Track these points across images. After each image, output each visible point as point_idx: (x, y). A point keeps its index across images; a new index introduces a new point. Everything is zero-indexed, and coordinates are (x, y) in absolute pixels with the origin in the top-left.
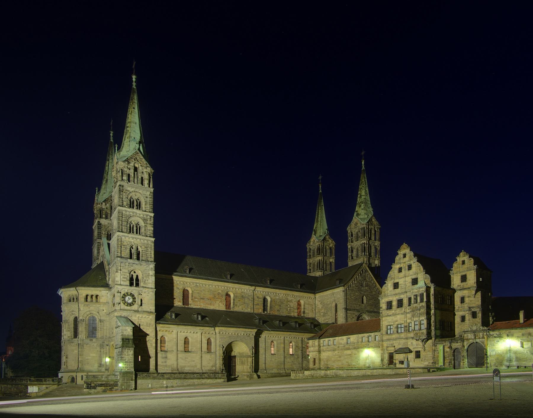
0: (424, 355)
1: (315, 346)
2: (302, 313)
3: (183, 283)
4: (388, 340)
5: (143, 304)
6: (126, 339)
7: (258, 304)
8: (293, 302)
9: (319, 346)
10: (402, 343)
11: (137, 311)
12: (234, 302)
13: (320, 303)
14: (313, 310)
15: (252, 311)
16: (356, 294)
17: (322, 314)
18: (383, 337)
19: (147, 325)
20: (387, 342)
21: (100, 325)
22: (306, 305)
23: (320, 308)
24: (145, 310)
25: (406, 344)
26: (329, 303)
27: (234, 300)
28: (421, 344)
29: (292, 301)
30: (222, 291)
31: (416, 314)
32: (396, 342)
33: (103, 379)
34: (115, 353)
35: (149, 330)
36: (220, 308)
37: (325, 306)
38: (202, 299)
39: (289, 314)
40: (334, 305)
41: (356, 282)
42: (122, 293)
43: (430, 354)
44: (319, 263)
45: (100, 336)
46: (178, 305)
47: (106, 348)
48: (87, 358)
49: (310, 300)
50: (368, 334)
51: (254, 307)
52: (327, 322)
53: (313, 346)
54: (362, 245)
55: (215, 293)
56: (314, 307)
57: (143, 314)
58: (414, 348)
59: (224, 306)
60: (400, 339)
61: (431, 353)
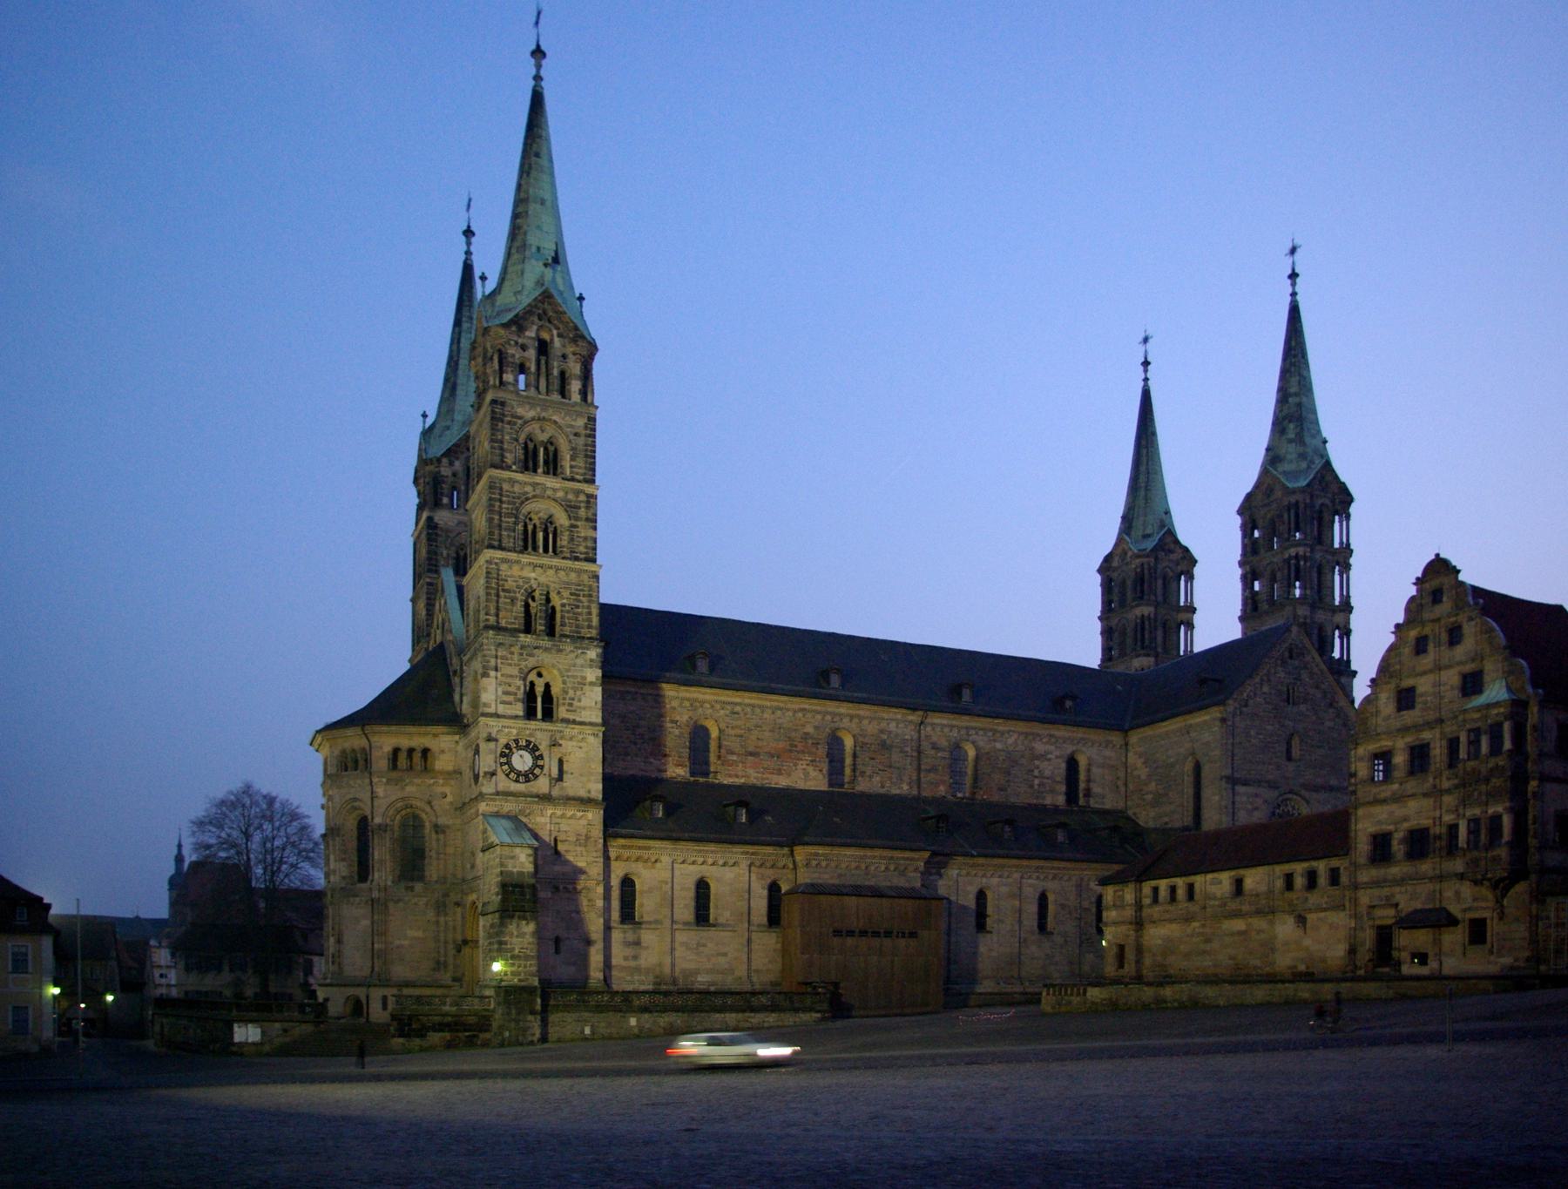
0: (1498, 934)
1: (1122, 907)
3: (692, 705)
4: (1376, 883)
5: (565, 776)
6: (516, 886)
7: (933, 769)
8: (1049, 760)
9: (1139, 906)
10: (1423, 895)
11: (546, 798)
12: (854, 765)
13: (1142, 760)
14: (1120, 783)
15: (915, 792)
16: (1269, 727)
17: (1149, 797)
18: (1359, 873)
19: (578, 842)
20: (1369, 891)
21: (434, 844)
22: (1094, 770)
23: (1143, 777)
24: (571, 793)
25: (1438, 896)
27: (855, 756)
28: (1490, 896)
29: (1049, 756)
30: (816, 728)
31: (1476, 794)
32: (1403, 889)
33: (447, 1008)
34: (481, 928)
35: (584, 858)
36: (809, 783)
38: (751, 754)
39: (1037, 798)
40: (1189, 766)
41: (1266, 689)
42: (503, 741)
43: (1520, 931)
44: (1139, 628)
45: (435, 877)
46: (674, 775)
47: (455, 913)
48: (397, 942)
49: (1108, 753)
51: (923, 780)
52: (1166, 823)
53: (1118, 903)
54: (1287, 561)
55: (793, 734)
56: (1121, 774)
57: (565, 804)
58: (1465, 910)
59: (821, 777)
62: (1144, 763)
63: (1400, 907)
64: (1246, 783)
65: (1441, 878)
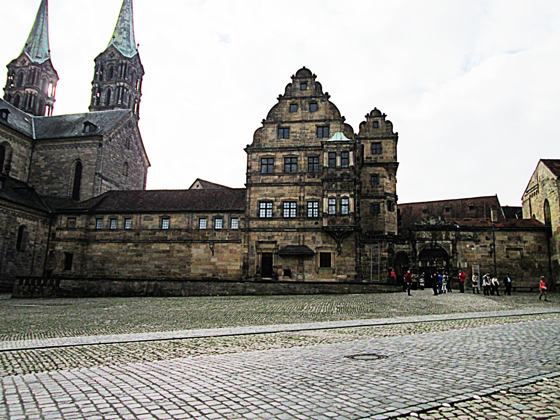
2: (4, 168)
4: (264, 229)
13: (43, 157)
14: (27, 168)
16: (118, 156)
17: (46, 178)
23: (43, 167)
25: (302, 238)
26: (64, 160)
32: (280, 234)
37: (55, 165)
40: (73, 166)
43: (350, 261)
49: (23, 148)
50: (215, 215)
56: (28, 163)
58: (317, 248)
60: (290, 229)
61: (352, 259)
62: (43, 159)
63: (278, 243)
64: (106, 180)
65: (304, 230)
